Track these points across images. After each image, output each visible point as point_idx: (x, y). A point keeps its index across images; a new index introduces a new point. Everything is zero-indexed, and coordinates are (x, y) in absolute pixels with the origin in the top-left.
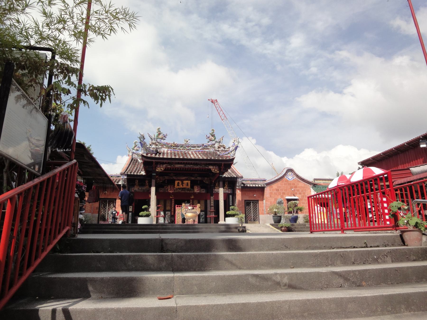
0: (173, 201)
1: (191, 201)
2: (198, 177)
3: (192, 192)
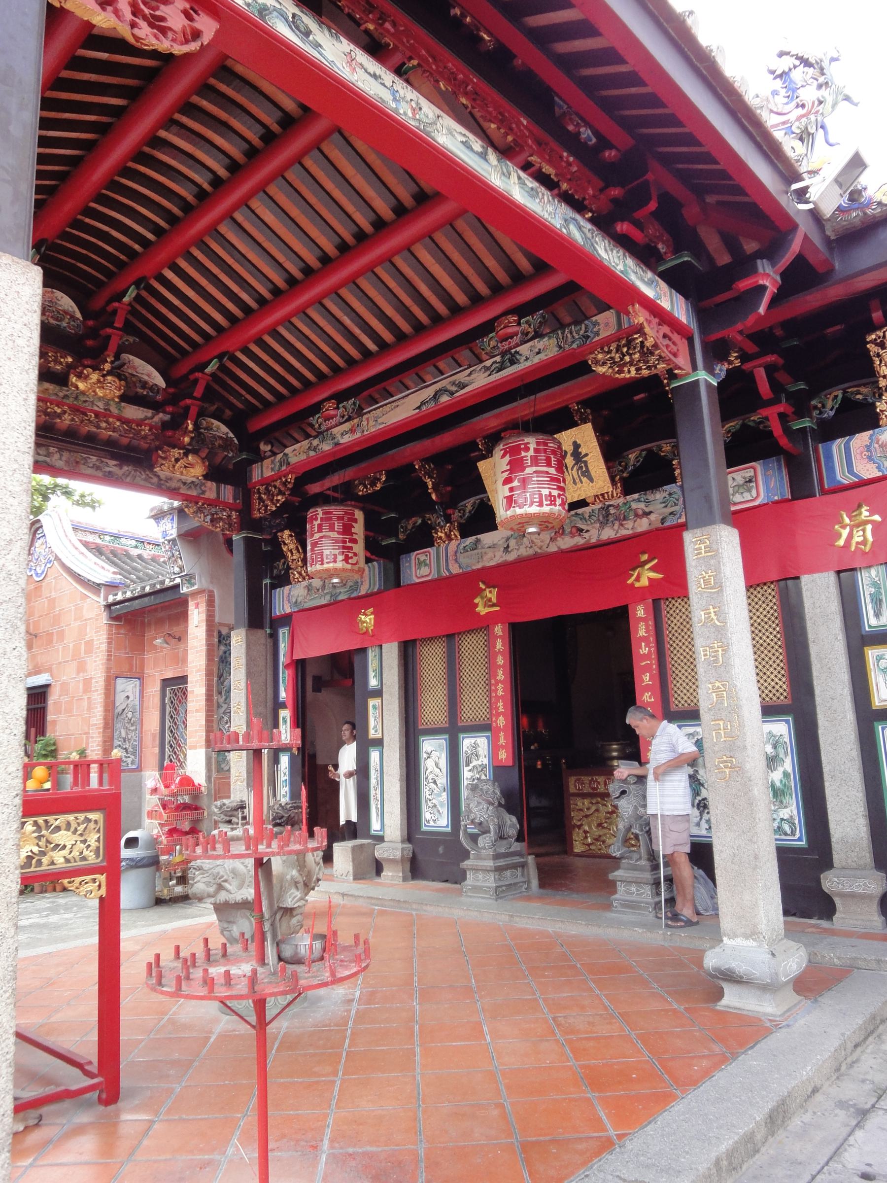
0: (499, 645)
1: (640, 612)
2: (524, 349)
3: (643, 525)
